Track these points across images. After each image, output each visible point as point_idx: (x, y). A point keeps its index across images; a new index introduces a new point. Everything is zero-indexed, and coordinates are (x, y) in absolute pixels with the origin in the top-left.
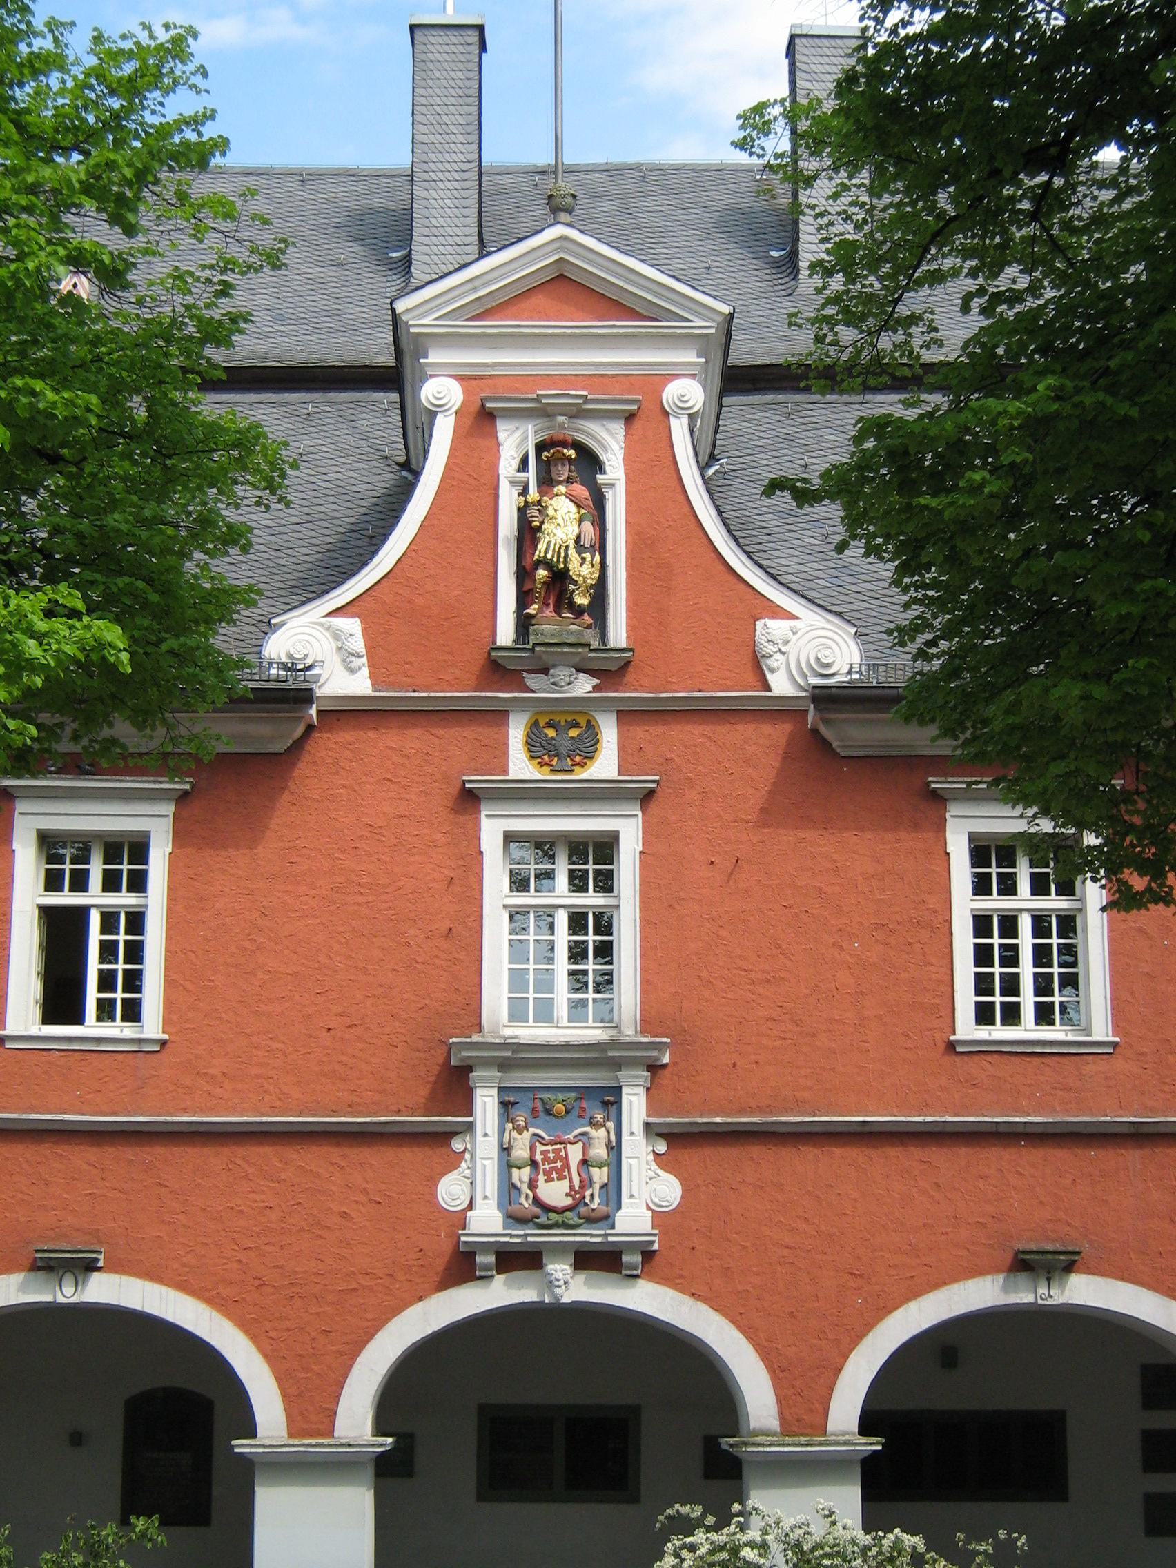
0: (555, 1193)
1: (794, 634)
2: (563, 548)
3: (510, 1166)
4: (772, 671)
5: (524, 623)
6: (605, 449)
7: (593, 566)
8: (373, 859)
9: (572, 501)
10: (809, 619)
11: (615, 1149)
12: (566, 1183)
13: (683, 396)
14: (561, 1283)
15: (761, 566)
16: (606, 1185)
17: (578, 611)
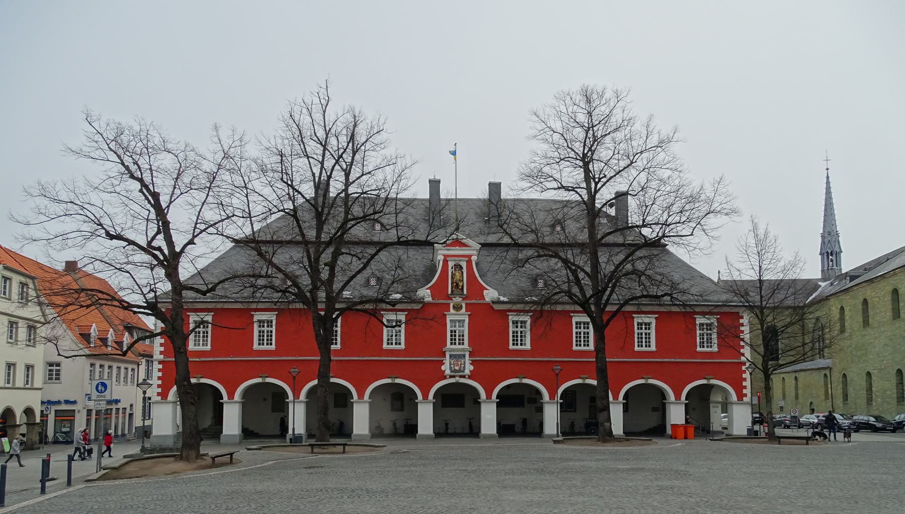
0: (457, 368)
5: (452, 291)
10: (491, 290)
11: (465, 362)
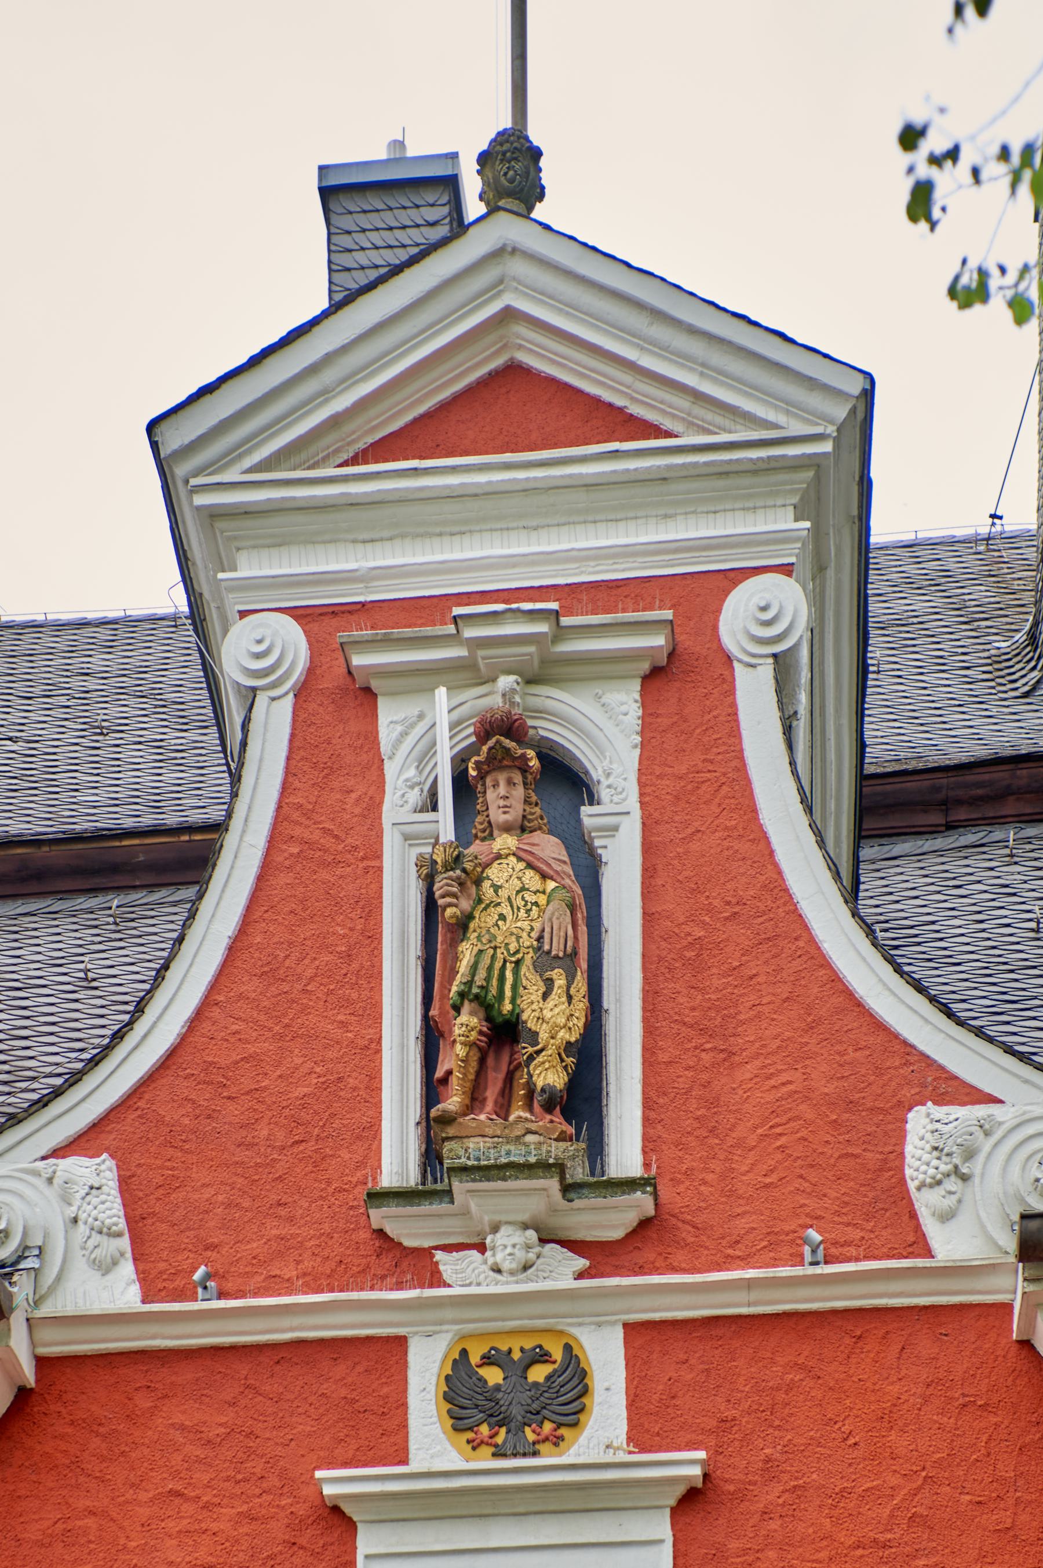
1: (987, 1134)
6: (600, 751)
9: (530, 866)
13: (764, 609)
15: (919, 987)
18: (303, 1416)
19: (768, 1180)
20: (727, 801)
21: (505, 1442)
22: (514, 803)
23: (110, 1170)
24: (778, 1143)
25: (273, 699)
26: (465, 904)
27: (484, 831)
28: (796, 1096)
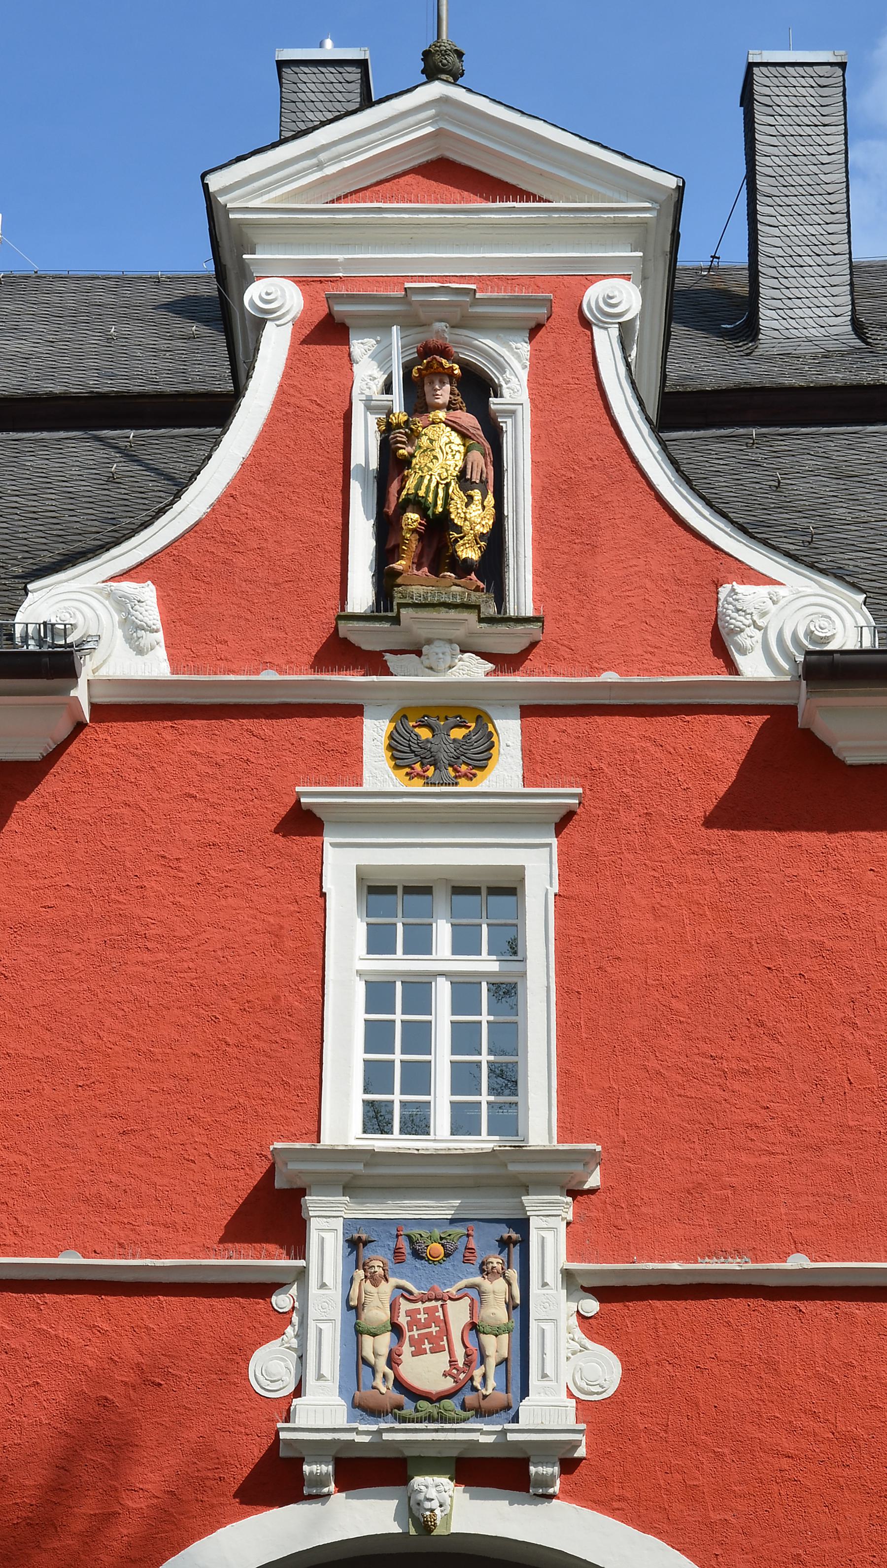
1: (774, 603)
2: (441, 487)
3: (359, 1332)
4: (743, 651)
7: (484, 507)
8: (166, 902)
9: (453, 429)
12: (445, 1357)
13: (611, 298)
14: (435, 1504)
16: (506, 1360)
17: (463, 568)
18: (287, 751)
19: (620, 623)
20: (589, 401)
21: (433, 775)
22: (443, 393)
23: (152, 591)
24: (628, 601)
25: (278, 326)
26: (410, 449)
27: (421, 408)
28: (640, 574)
